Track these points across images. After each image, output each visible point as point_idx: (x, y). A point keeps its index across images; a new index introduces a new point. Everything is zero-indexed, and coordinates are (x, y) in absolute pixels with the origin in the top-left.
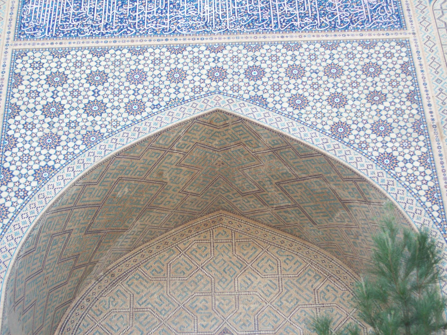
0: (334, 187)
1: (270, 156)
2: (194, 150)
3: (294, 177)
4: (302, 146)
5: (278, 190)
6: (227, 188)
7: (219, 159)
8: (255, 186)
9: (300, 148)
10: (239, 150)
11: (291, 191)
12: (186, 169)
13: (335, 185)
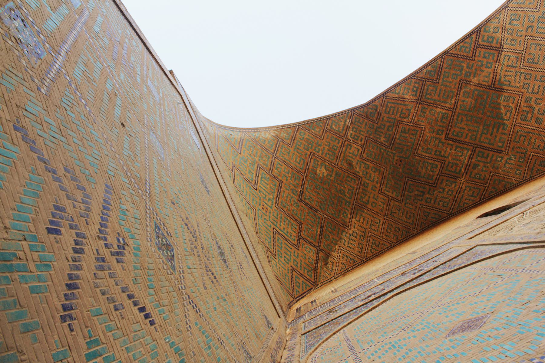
0: (475, 80)
1: (422, 111)
2: (368, 144)
3: (450, 113)
4: (429, 68)
5: (452, 145)
6: (421, 190)
7: (396, 158)
8: (436, 163)
9: (429, 72)
10: (402, 132)
11: (460, 134)
12: (371, 165)
13: (474, 77)
